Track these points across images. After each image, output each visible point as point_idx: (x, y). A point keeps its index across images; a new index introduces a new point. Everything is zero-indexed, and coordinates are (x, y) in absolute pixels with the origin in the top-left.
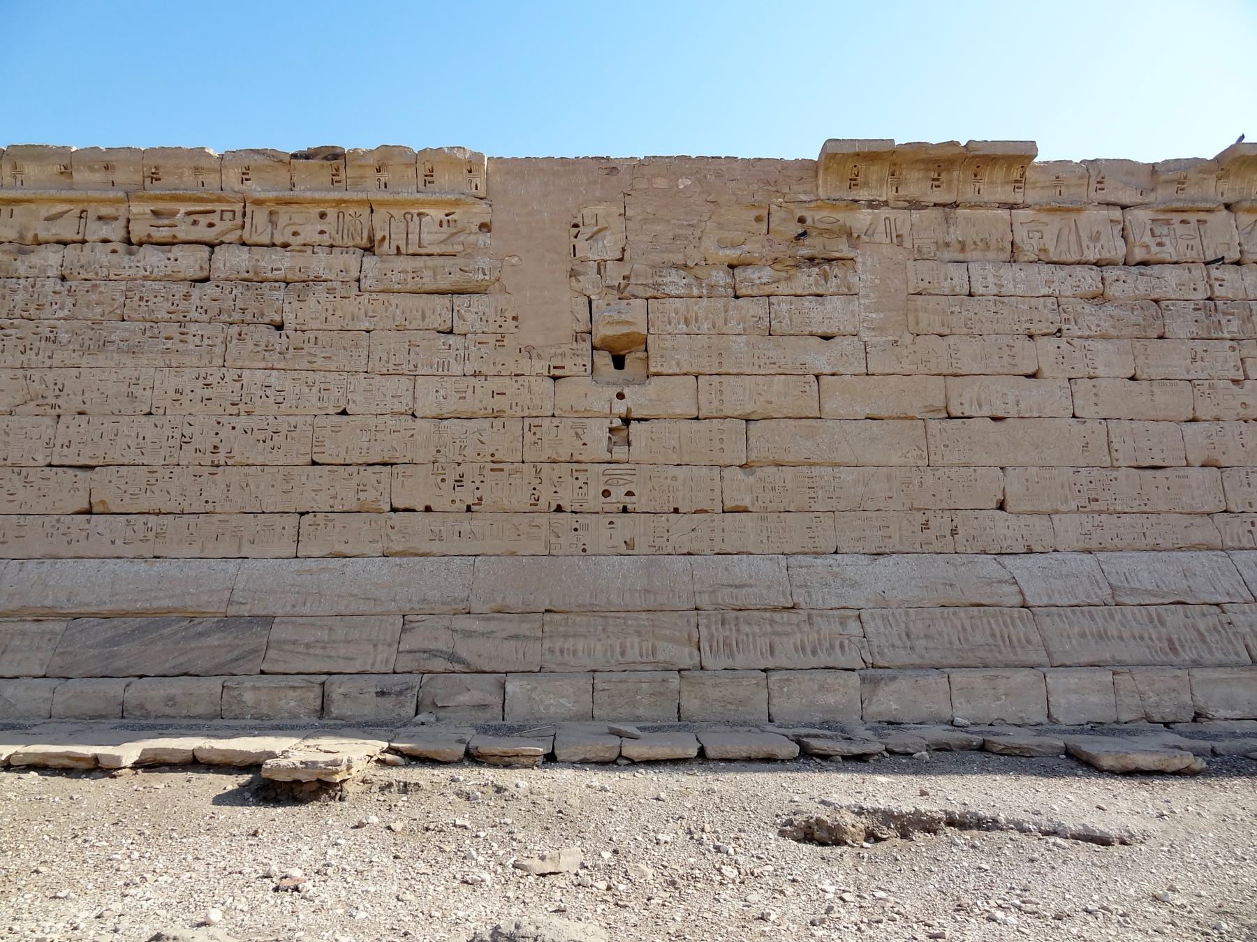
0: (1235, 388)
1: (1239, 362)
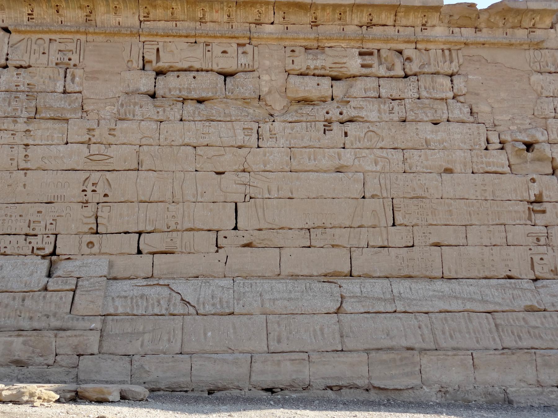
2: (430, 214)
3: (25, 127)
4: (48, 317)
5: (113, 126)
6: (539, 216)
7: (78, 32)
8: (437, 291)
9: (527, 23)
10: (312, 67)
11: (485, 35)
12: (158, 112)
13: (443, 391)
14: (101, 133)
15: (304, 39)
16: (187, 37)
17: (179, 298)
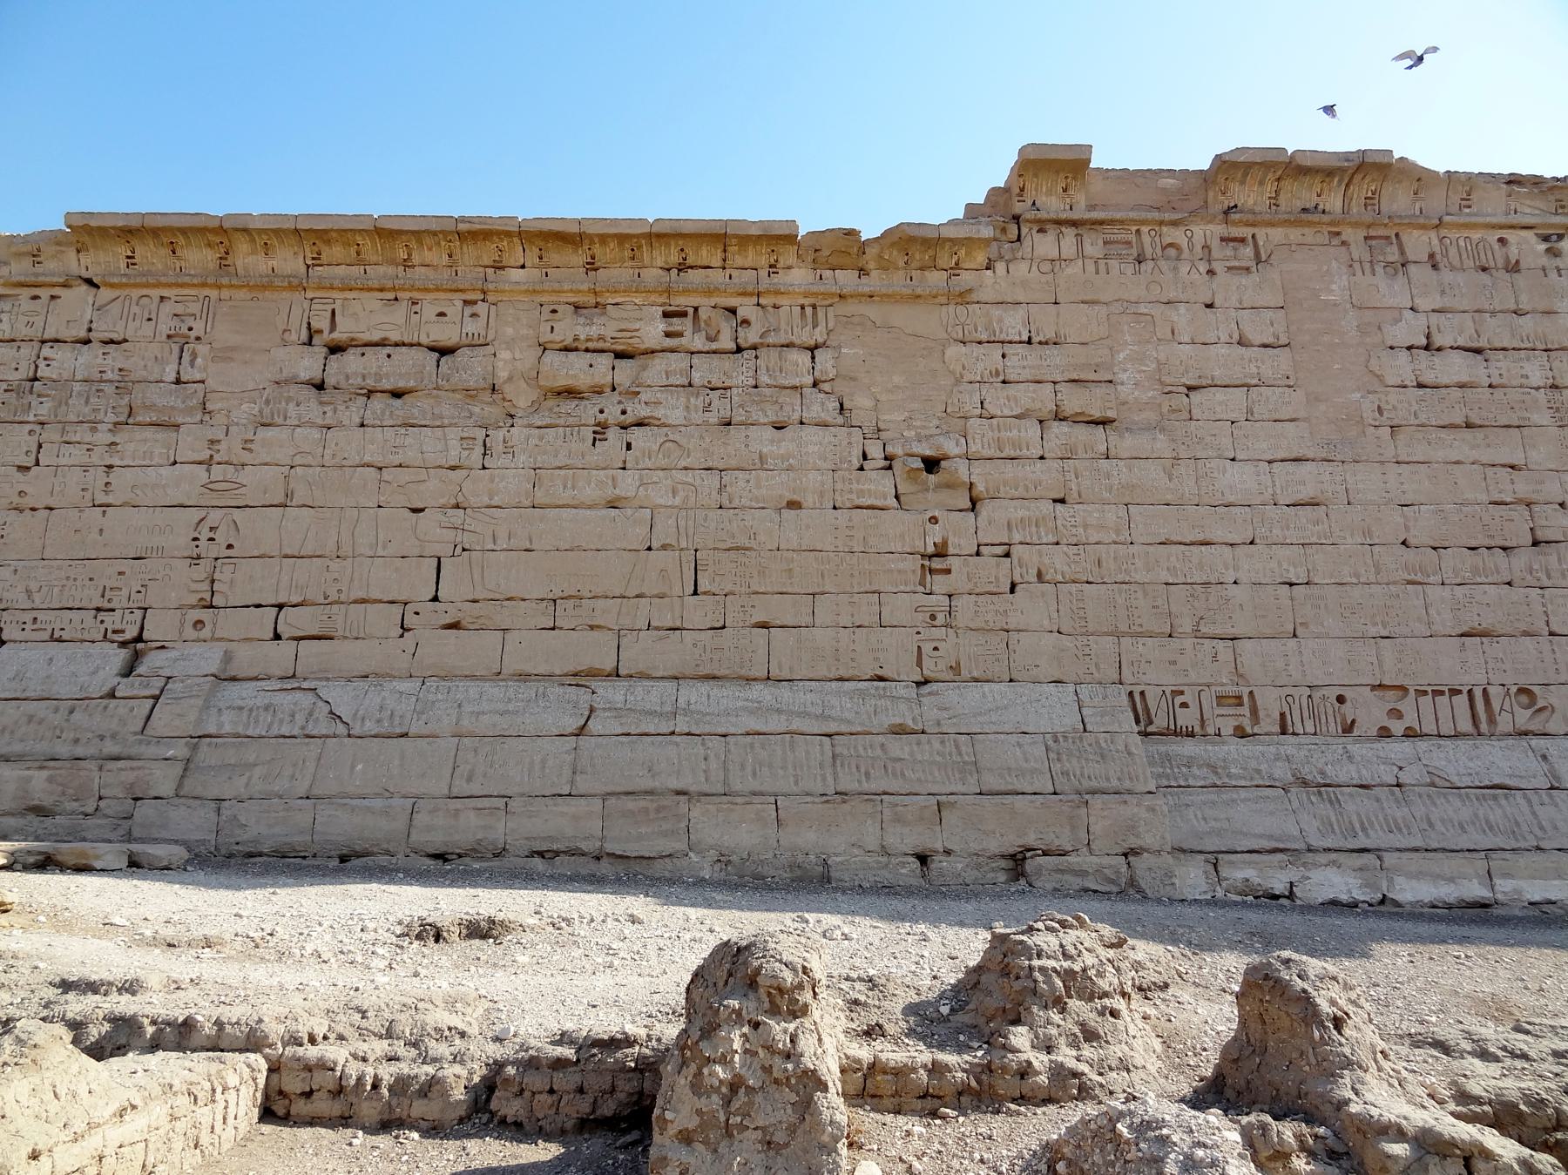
0: (19, 475)
1: (34, 449)
2: (755, 574)
3: (110, 438)
4: (102, 738)
5: (250, 436)
6: (938, 578)
7: (204, 285)
8: (751, 701)
9: (945, 260)
10: (582, 337)
11: (875, 282)
12: (325, 413)
13: (723, 860)
14: (230, 448)
15: (571, 291)
16: (381, 290)
17: (326, 709)
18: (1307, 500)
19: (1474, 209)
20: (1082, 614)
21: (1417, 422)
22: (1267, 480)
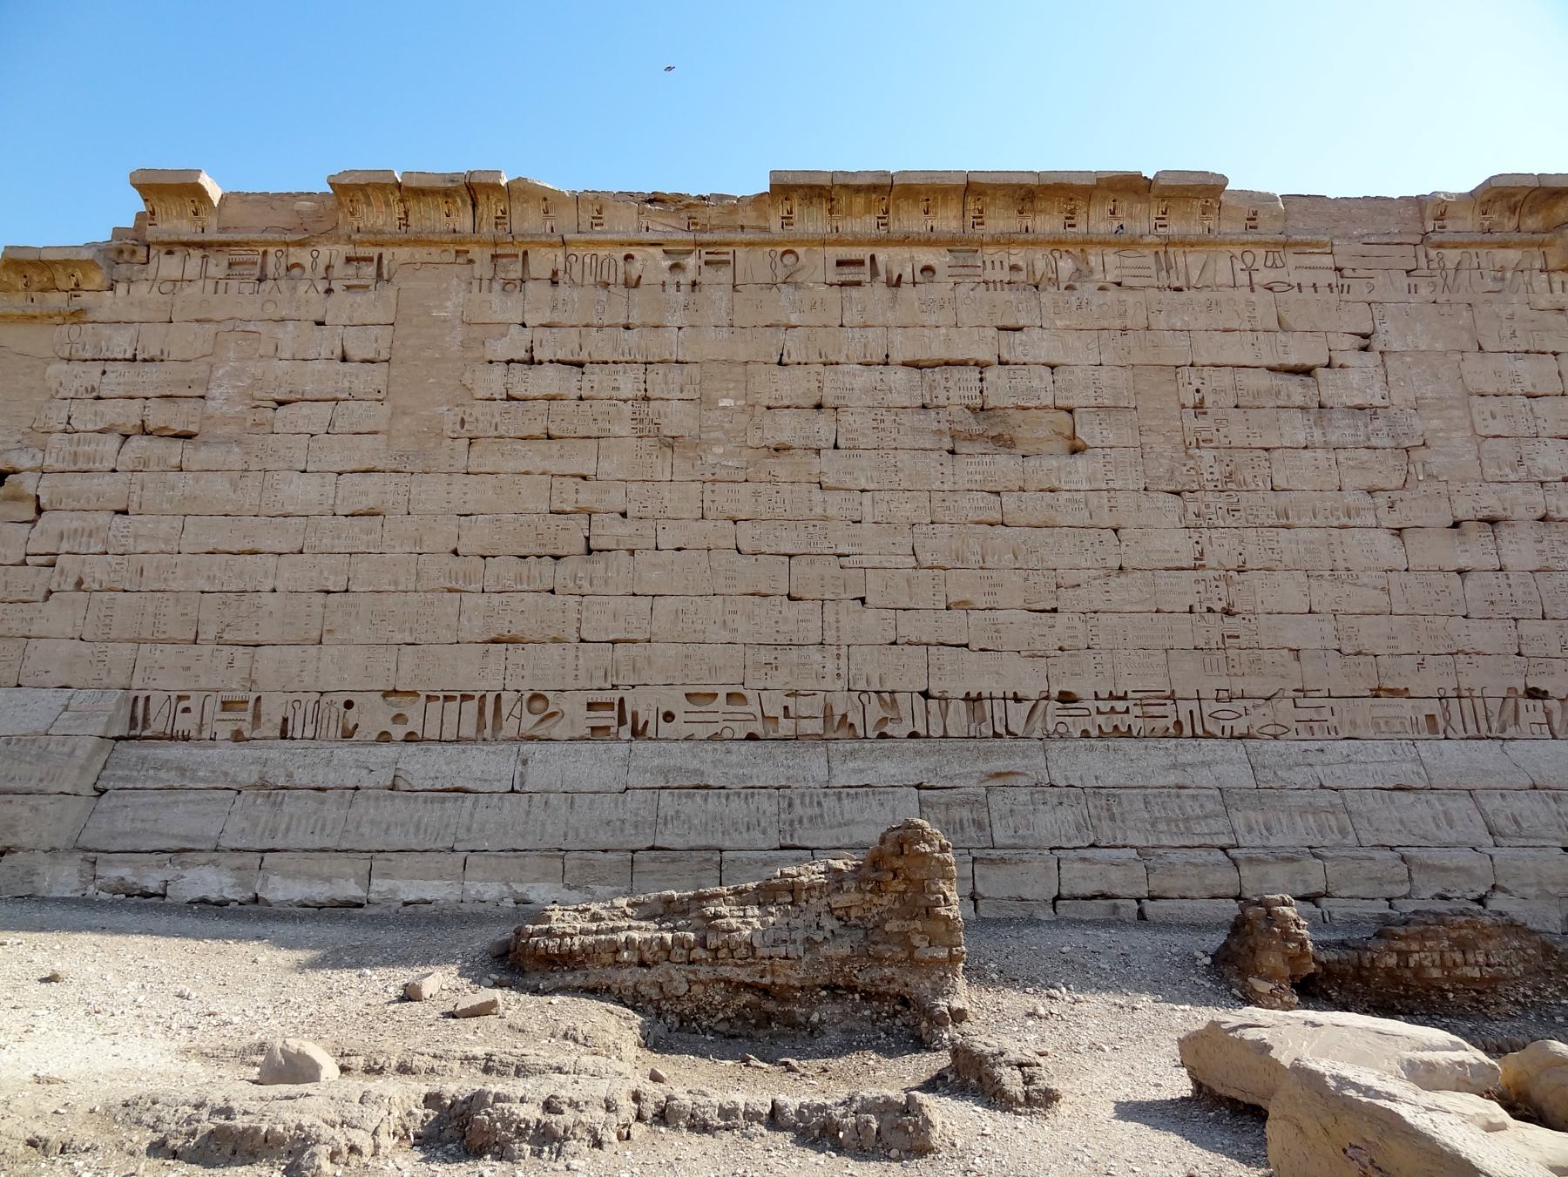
18: (365, 510)
19: (606, 227)
20: (108, 621)
21: (496, 434)
22: (330, 491)
